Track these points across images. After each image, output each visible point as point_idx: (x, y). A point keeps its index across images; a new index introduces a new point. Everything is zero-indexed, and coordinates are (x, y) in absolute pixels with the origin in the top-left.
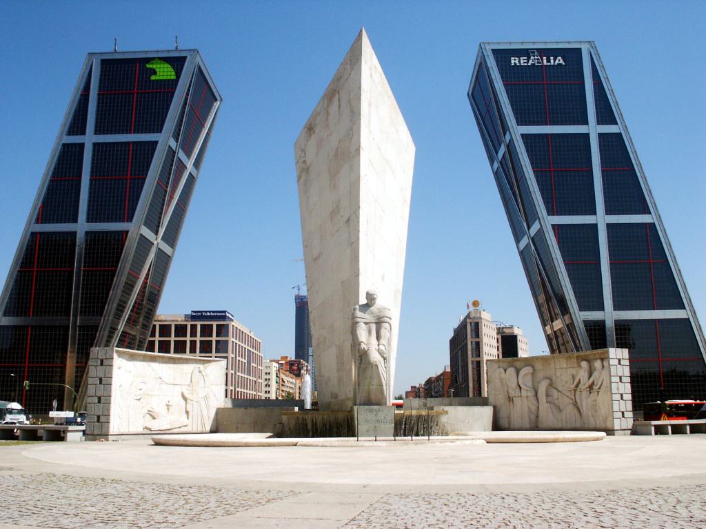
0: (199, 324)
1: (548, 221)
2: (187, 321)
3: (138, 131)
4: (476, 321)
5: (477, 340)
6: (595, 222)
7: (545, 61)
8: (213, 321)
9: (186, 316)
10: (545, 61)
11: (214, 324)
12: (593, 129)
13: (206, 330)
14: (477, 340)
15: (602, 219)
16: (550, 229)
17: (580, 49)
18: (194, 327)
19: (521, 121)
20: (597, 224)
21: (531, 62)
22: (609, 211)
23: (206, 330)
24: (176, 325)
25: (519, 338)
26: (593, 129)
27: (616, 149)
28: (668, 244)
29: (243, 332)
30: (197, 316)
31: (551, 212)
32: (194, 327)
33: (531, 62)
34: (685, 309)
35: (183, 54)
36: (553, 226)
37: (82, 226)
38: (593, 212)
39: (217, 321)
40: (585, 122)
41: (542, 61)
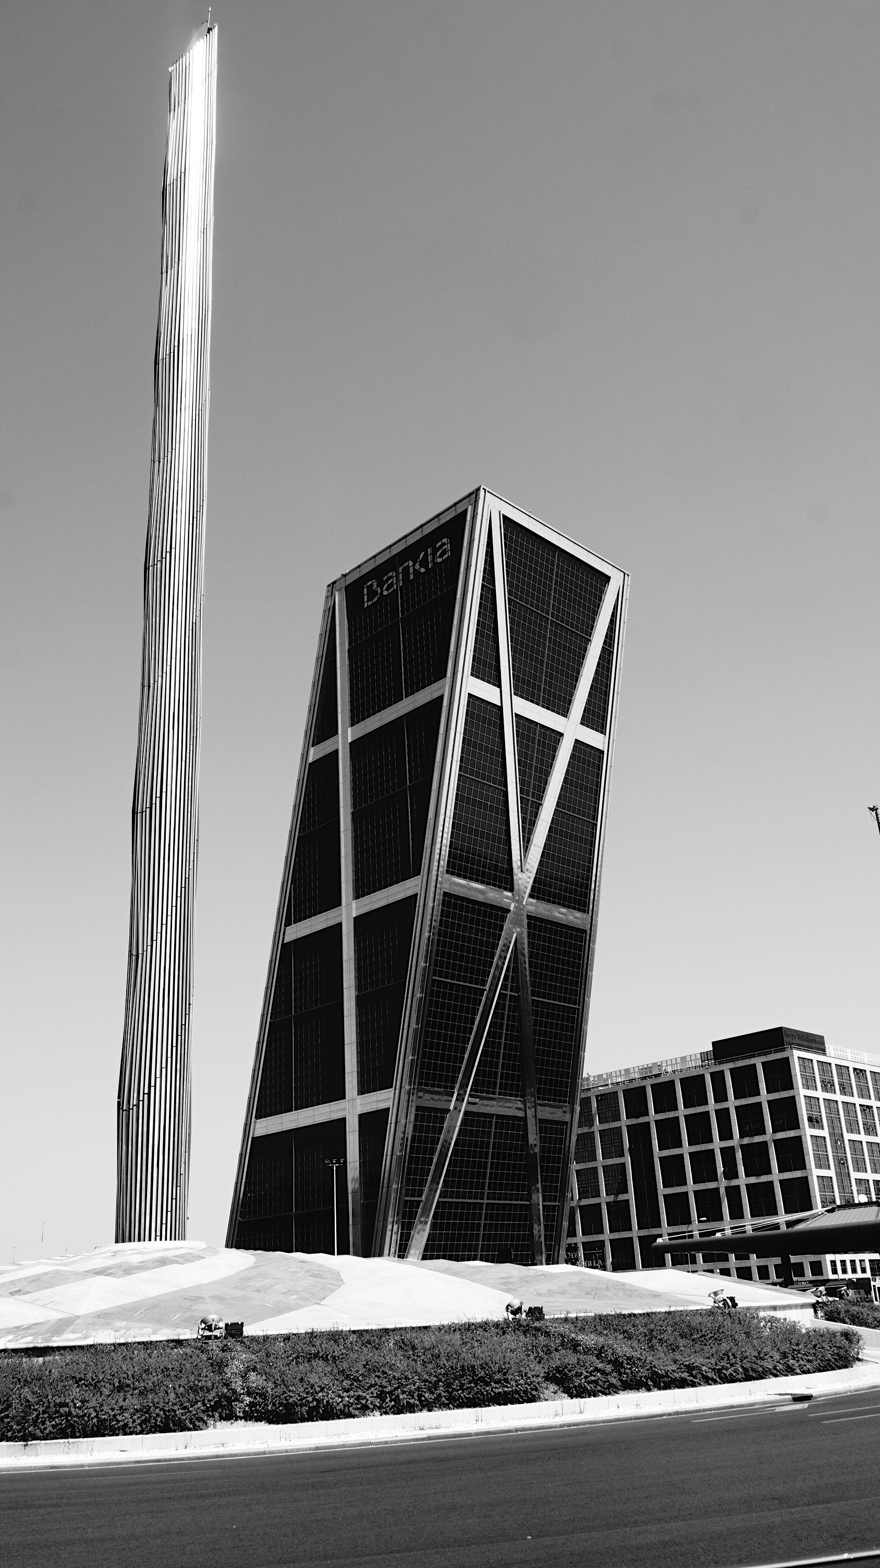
0: (726, 1068)
2: (721, 1063)
3: (411, 692)
8: (754, 1056)
9: (704, 1056)
11: (758, 1062)
13: (745, 1083)
18: (718, 1078)
23: (745, 1083)
24: (682, 1080)
29: (859, 1072)
30: (724, 1049)
32: (718, 1078)
35: (460, 509)
37: (350, 909)
39: (765, 1054)
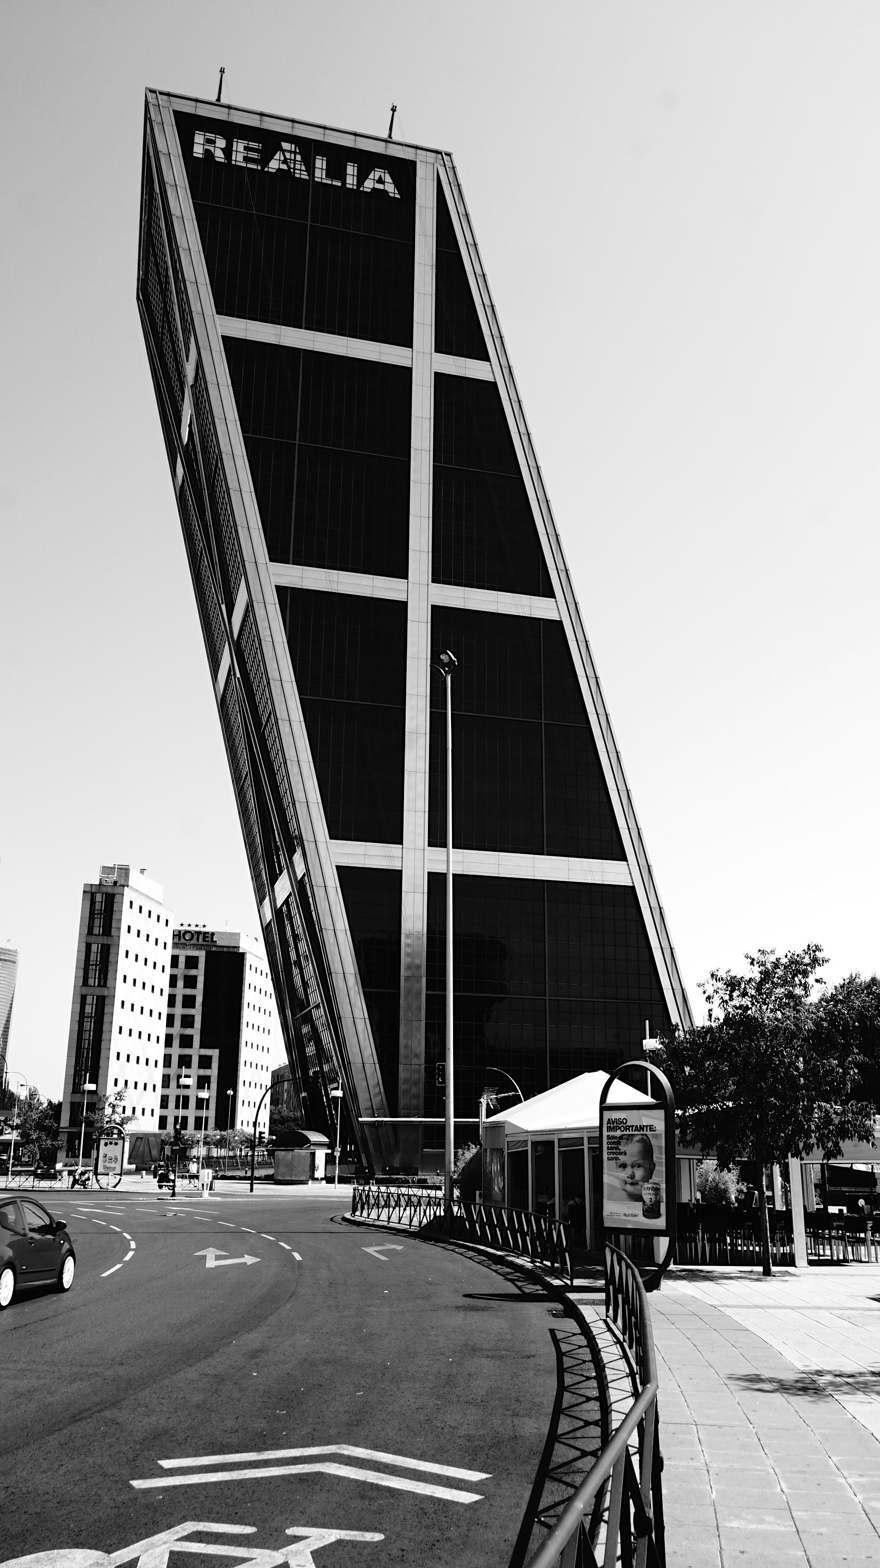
1: (267, 577)
4: (110, 890)
5: (105, 940)
6: (401, 597)
7: (320, 175)
10: (320, 175)
12: (424, 360)
14: (105, 940)
15: (420, 592)
16: (272, 598)
17: (414, 163)
19: (224, 307)
20: (403, 606)
22: (440, 575)
25: (249, 961)
26: (424, 360)
28: (593, 682)
31: (277, 554)
33: (274, 165)
34: (625, 859)
36: (279, 589)
38: (400, 570)
40: (406, 340)
41: (311, 169)
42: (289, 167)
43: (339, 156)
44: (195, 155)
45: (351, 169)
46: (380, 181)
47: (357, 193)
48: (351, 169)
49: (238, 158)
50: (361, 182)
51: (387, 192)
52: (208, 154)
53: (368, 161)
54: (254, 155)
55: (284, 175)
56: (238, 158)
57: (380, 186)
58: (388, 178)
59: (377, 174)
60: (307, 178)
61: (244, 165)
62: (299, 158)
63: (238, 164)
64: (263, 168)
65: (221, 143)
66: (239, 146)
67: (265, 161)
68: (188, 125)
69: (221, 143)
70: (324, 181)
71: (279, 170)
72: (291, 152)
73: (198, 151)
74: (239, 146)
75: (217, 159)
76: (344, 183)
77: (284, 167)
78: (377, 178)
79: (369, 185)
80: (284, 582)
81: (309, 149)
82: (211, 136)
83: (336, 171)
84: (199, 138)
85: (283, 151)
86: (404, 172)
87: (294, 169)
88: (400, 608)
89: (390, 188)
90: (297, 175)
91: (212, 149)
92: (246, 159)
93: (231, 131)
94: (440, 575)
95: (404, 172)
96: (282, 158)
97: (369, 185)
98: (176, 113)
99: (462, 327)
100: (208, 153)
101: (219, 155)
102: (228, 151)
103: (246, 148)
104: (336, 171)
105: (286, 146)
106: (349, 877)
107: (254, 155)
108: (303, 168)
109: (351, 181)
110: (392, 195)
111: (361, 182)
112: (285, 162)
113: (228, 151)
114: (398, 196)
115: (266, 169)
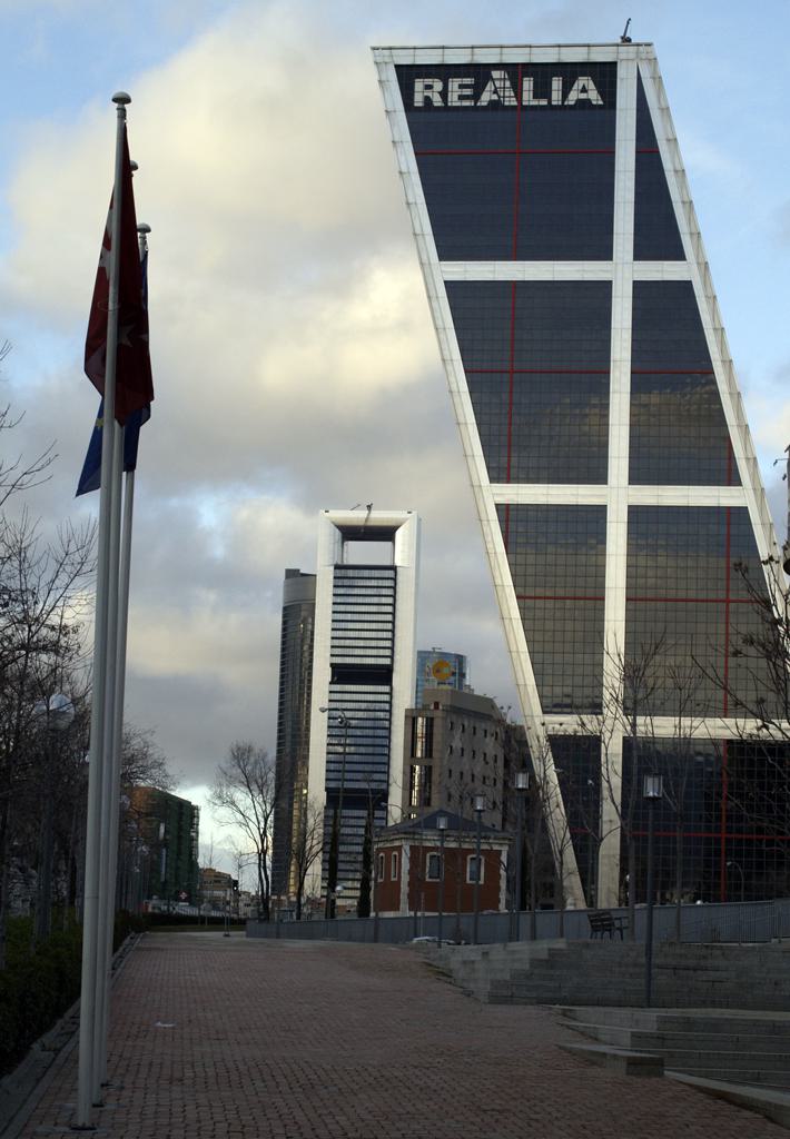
10: (528, 98)
15: (618, 495)
16: (493, 515)
21: (486, 97)
27: (672, 320)
33: (486, 97)
42: (499, 97)
43: (541, 73)
44: (416, 105)
45: (557, 84)
46: (584, 90)
47: (563, 107)
48: (557, 84)
49: (453, 100)
50: (565, 95)
51: (589, 100)
52: (428, 100)
53: (570, 72)
54: (468, 92)
55: (495, 105)
56: (453, 100)
57: (583, 96)
58: (591, 85)
59: (582, 81)
60: (515, 103)
61: (458, 104)
62: (508, 84)
63: (454, 104)
64: (476, 103)
65: (438, 86)
66: (454, 84)
67: (476, 96)
68: (407, 75)
69: (438, 86)
70: (531, 103)
71: (491, 102)
72: (500, 79)
73: (418, 100)
74: (454, 84)
75: (436, 104)
76: (550, 101)
77: (495, 97)
78: (580, 88)
79: (573, 96)
80: (502, 500)
81: (516, 72)
82: (428, 81)
83: (542, 90)
84: (419, 85)
85: (493, 80)
86: (605, 74)
87: (504, 97)
88: (601, 511)
89: (594, 96)
90: (506, 104)
91: (430, 95)
92: (461, 98)
93: (444, 72)
94: (637, 477)
95: (605, 74)
96: (493, 88)
97: (573, 96)
98: (396, 66)
99: (660, 232)
100: (428, 100)
101: (437, 101)
102: (444, 94)
103: (461, 86)
104: (542, 90)
105: (496, 74)
106: (558, 743)
107: (468, 92)
108: (512, 94)
109: (556, 97)
110: (594, 103)
111: (565, 95)
112: (496, 92)
113: (444, 94)
114: (601, 103)
115: (479, 104)
